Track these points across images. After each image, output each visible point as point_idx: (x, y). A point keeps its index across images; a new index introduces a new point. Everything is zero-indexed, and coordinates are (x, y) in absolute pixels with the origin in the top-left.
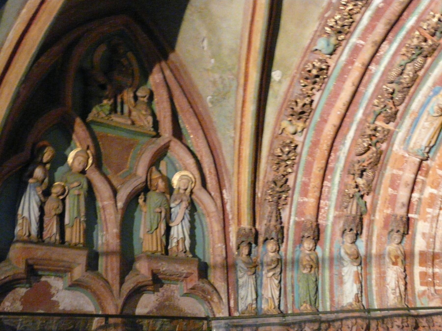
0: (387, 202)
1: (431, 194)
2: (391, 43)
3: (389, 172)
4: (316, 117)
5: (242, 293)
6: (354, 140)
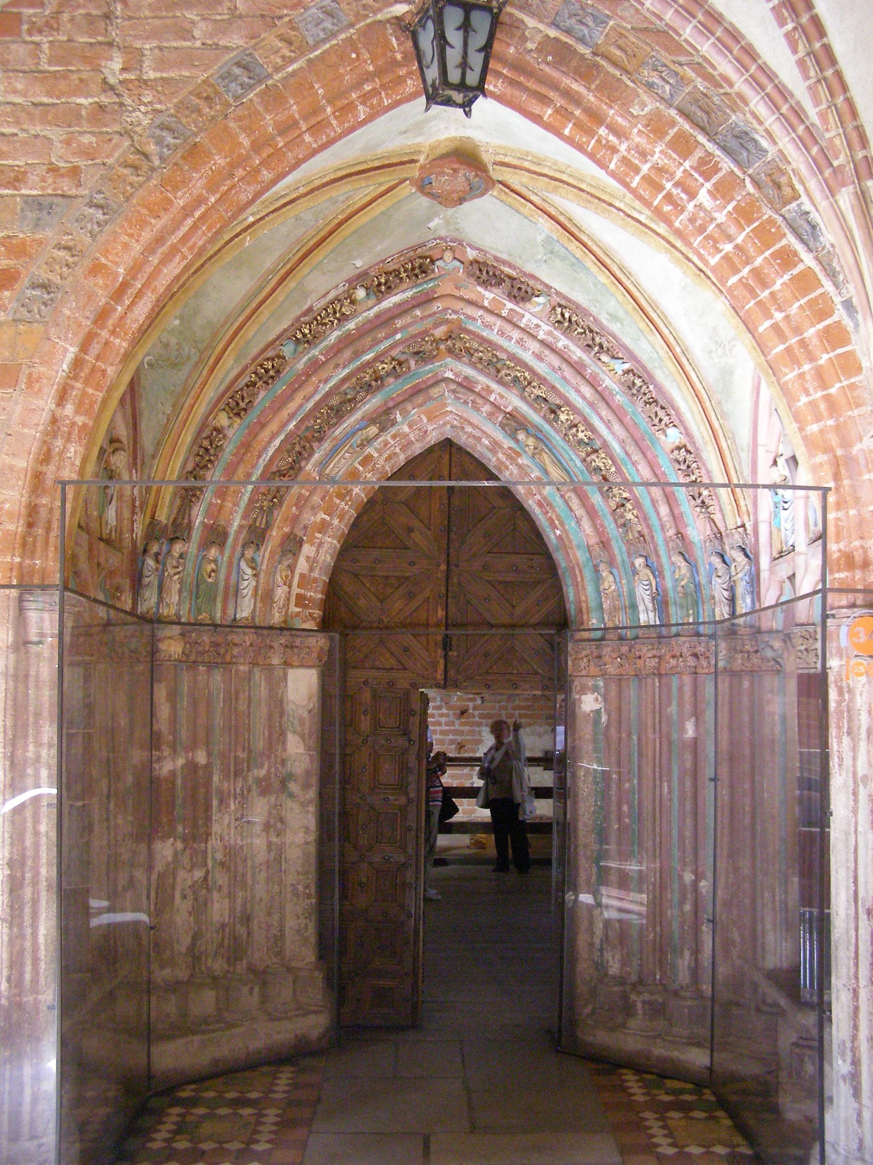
1: (323, 519)
4: (252, 416)
5: (147, 594)
6: (278, 450)
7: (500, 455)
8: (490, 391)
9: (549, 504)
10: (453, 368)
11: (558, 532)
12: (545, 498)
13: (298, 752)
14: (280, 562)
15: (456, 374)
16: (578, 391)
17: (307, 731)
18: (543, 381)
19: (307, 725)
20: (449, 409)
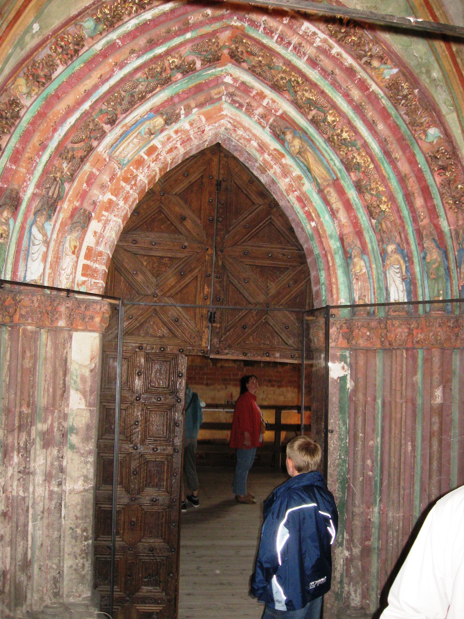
0: (79, 196)
2: (138, 57)
3: (87, 167)
4: (52, 88)
6: (74, 127)
7: (266, 156)
8: (262, 96)
9: (308, 199)
10: (232, 73)
11: (313, 224)
12: (304, 194)
13: (79, 408)
14: (69, 234)
15: (235, 80)
16: (347, 96)
17: (88, 389)
18: (314, 85)
19: (89, 383)
20: (224, 113)
